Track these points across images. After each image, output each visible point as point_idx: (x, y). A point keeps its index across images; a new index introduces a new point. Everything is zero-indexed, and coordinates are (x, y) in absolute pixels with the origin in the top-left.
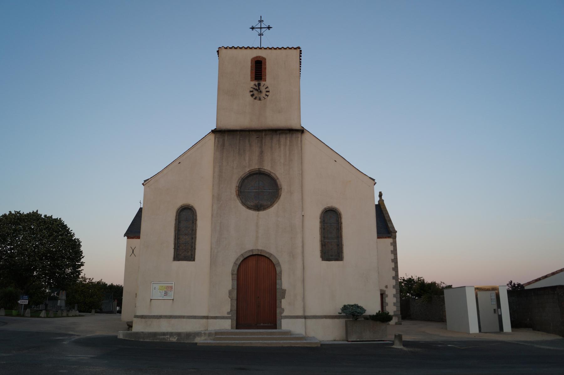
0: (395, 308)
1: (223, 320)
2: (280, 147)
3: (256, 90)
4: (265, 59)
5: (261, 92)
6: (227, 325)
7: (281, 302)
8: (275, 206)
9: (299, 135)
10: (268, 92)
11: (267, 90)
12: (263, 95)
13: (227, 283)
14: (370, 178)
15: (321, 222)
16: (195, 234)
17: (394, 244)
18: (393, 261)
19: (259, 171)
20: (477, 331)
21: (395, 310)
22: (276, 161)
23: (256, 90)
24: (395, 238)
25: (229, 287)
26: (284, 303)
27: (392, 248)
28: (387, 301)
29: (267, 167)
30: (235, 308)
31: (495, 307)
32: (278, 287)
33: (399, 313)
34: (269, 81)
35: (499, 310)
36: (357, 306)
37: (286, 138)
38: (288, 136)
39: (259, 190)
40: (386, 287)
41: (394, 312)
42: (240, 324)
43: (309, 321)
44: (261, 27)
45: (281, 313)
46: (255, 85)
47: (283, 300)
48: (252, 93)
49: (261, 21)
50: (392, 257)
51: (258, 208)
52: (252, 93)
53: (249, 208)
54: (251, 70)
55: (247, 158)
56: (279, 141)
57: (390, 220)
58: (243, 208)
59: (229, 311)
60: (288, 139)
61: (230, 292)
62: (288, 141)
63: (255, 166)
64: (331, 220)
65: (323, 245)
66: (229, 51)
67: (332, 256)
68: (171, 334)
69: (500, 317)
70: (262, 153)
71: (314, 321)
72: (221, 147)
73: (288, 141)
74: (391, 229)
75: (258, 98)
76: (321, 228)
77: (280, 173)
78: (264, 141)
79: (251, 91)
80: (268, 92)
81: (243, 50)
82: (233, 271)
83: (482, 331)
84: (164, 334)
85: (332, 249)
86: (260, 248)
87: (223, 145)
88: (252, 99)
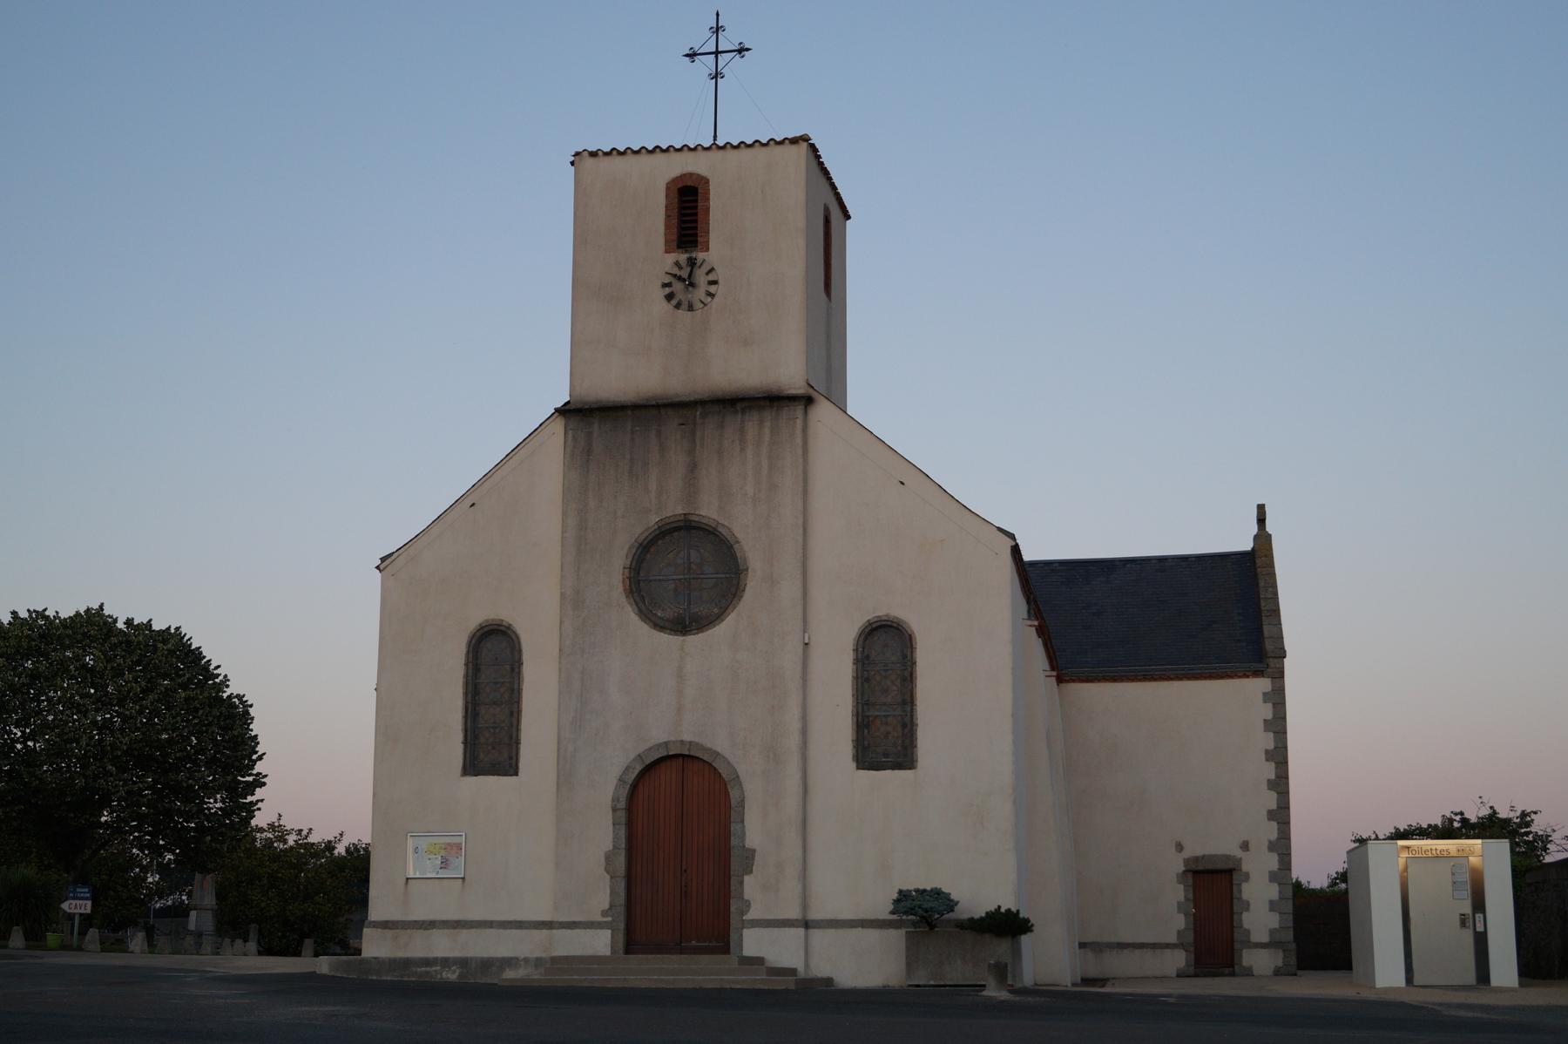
0: (1273, 921)
1: (590, 932)
2: (742, 450)
3: (680, 279)
4: (707, 181)
5: (692, 285)
6: (600, 943)
7: (742, 883)
8: (730, 619)
9: (799, 410)
10: (715, 283)
11: (711, 277)
12: (700, 293)
13: (601, 834)
14: (1000, 529)
15: (857, 661)
16: (519, 702)
17: (1277, 698)
18: (1269, 756)
19: (686, 521)
20: (1399, 980)
21: (1276, 925)
22: (734, 491)
23: (680, 279)
24: (1279, 675)
25: (608, 844)
26: (751, 886)
27: (1267, 712)
28: (1245, 896)
29: (708, 510)
30: (621, 899)
31: (1467, 908)
32: (734, 841)
33: (1290, 936)
34: (716, 251)
35: (1479, 917)
36: (937, 893)
37: (761, 422)
38: (768, 415)
39: (686, 577)
40: (1245, 846)
41: (1272, 932)
42: (633, 941)
43: (817, 935)
44: (717, 53)
45: (743, 913)
46: (677, 264)
47: (746, 878)
48: (668, 290)
49: (717, 30)
50: (1268, 741)
51: (684, 625)
52: (668, 290)
53: (659, 626)
54: (668, 216)
55: (653, 486)
56: (742, 431)
57: (1276, 612)
58: (644, 629)
59: (607, 906)
60: (768, 424)
61: (609, 858)
62: (767, 431)
63: (675, 508)
64: (885, 653)
65: (862, 724)
66: (604, 162)
67: (886, 755)
68: (445, 962)
69: (1481, 941)
70: (693, 467)
71: (831, 933)
72: (581, 457)
73: (767, 431)
74: (1269, 646)
75: (685, 305)
76: (856, 678)
77: (742, 524)
78: (698, 434)
79: (665, 285)
80: (715, 283)
81: (644, 158)
82: (615, 799)
83: (1417, 980)
84: (428, 962)
85: (885, 737)
86: (687, 737)
87: (588, 451)
88: (667, 307)
